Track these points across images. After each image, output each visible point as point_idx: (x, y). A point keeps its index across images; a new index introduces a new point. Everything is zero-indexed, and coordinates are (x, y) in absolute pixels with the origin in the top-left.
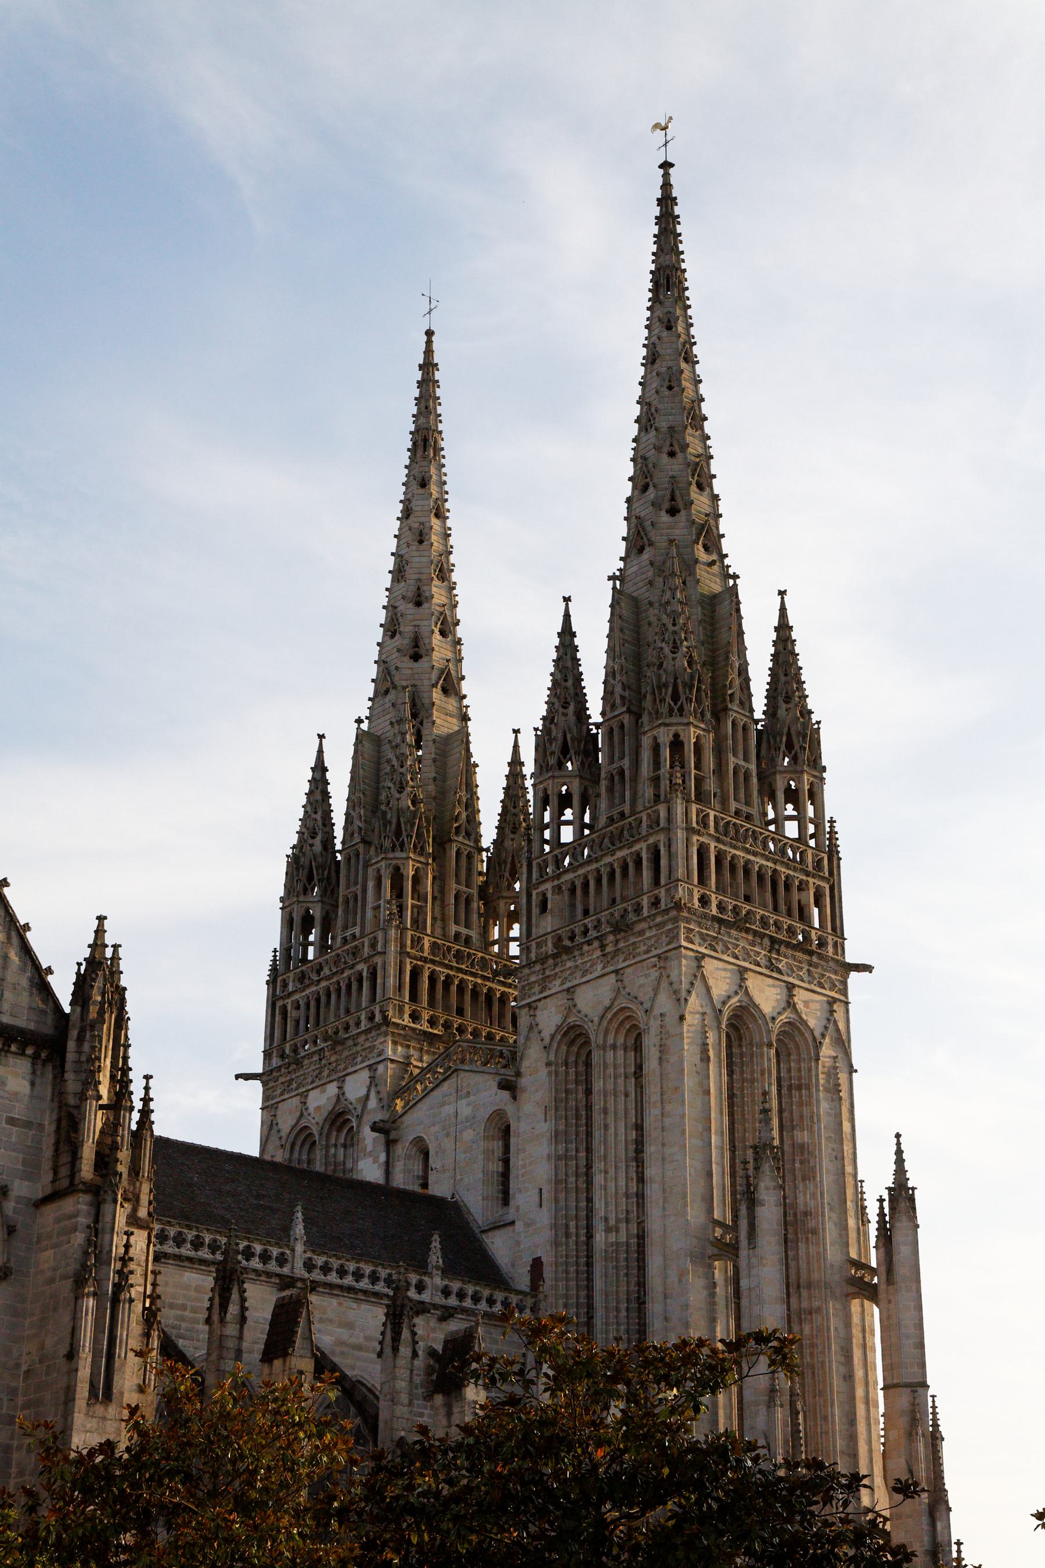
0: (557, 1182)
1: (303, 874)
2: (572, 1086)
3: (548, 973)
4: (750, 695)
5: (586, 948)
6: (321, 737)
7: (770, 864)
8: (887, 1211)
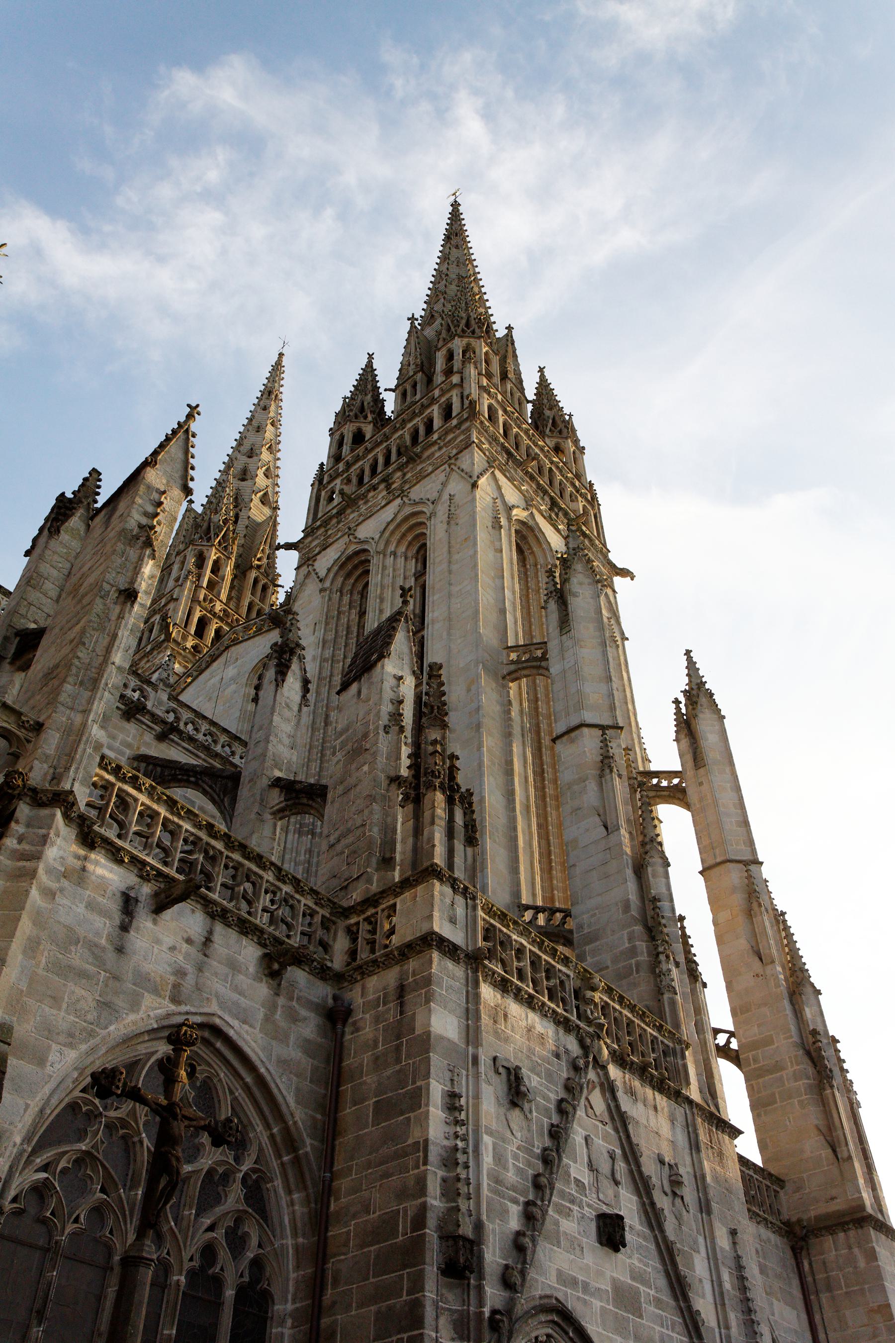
3: (329, 532)
8: (684, 711)
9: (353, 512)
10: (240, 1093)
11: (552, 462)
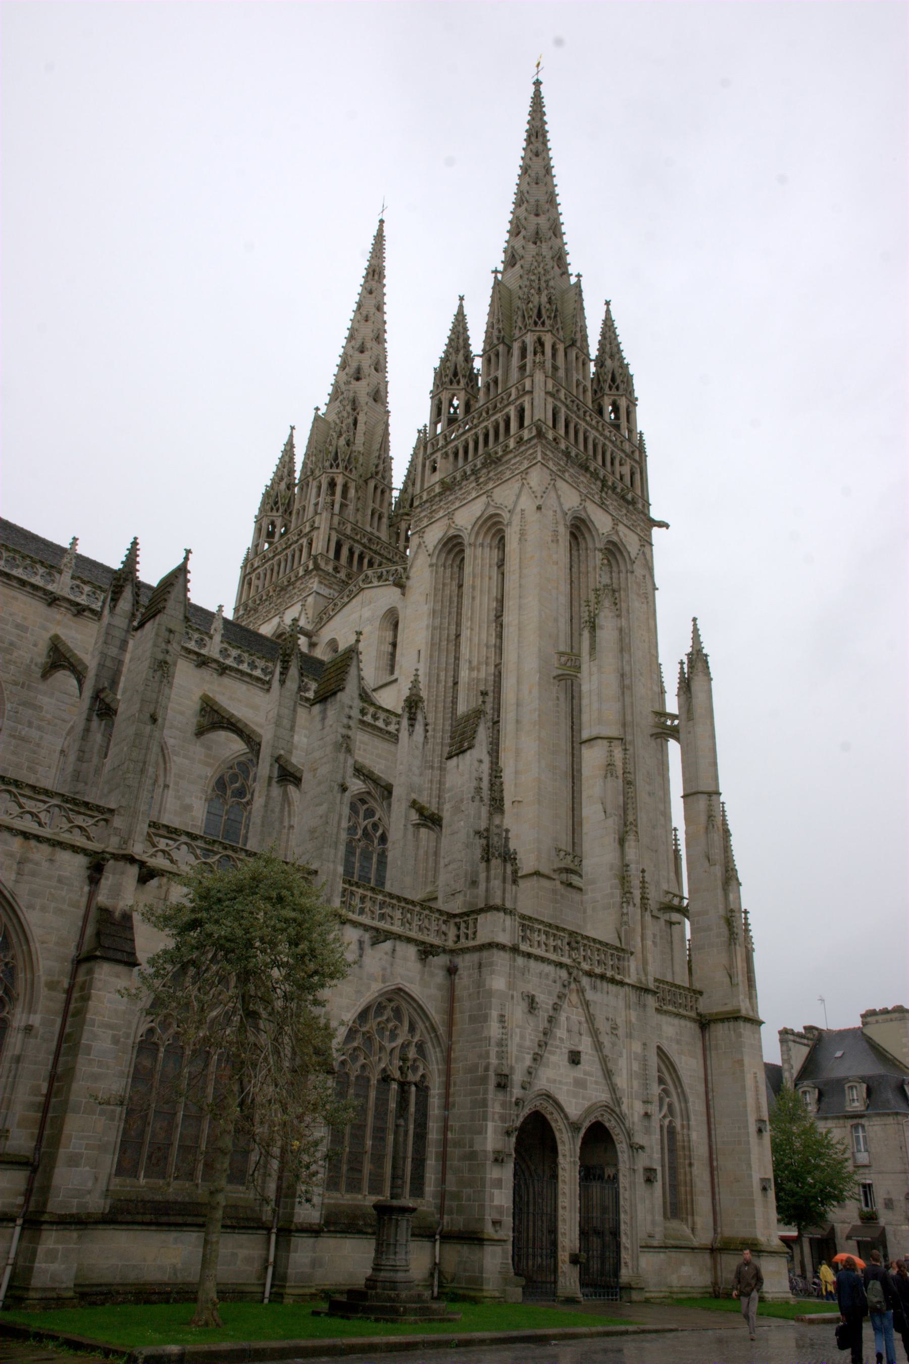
0: (432, 645)
1: (271, 501)
2: (448, 581)
3: (434, 507)
4: (588, 346)
5: (464, 483)
6: (293, 428)
7: (602, 438)
8: (686, 670)
9: (451, 494)
10: (411, 1010)
11: (606, 438)
